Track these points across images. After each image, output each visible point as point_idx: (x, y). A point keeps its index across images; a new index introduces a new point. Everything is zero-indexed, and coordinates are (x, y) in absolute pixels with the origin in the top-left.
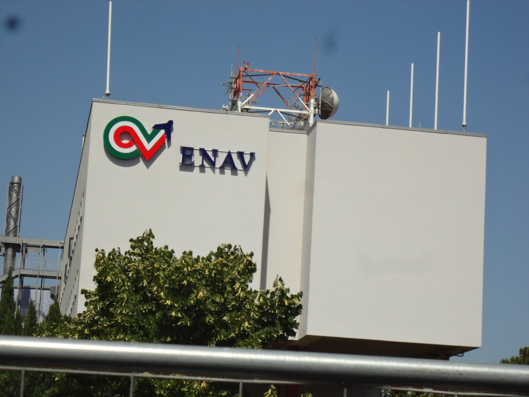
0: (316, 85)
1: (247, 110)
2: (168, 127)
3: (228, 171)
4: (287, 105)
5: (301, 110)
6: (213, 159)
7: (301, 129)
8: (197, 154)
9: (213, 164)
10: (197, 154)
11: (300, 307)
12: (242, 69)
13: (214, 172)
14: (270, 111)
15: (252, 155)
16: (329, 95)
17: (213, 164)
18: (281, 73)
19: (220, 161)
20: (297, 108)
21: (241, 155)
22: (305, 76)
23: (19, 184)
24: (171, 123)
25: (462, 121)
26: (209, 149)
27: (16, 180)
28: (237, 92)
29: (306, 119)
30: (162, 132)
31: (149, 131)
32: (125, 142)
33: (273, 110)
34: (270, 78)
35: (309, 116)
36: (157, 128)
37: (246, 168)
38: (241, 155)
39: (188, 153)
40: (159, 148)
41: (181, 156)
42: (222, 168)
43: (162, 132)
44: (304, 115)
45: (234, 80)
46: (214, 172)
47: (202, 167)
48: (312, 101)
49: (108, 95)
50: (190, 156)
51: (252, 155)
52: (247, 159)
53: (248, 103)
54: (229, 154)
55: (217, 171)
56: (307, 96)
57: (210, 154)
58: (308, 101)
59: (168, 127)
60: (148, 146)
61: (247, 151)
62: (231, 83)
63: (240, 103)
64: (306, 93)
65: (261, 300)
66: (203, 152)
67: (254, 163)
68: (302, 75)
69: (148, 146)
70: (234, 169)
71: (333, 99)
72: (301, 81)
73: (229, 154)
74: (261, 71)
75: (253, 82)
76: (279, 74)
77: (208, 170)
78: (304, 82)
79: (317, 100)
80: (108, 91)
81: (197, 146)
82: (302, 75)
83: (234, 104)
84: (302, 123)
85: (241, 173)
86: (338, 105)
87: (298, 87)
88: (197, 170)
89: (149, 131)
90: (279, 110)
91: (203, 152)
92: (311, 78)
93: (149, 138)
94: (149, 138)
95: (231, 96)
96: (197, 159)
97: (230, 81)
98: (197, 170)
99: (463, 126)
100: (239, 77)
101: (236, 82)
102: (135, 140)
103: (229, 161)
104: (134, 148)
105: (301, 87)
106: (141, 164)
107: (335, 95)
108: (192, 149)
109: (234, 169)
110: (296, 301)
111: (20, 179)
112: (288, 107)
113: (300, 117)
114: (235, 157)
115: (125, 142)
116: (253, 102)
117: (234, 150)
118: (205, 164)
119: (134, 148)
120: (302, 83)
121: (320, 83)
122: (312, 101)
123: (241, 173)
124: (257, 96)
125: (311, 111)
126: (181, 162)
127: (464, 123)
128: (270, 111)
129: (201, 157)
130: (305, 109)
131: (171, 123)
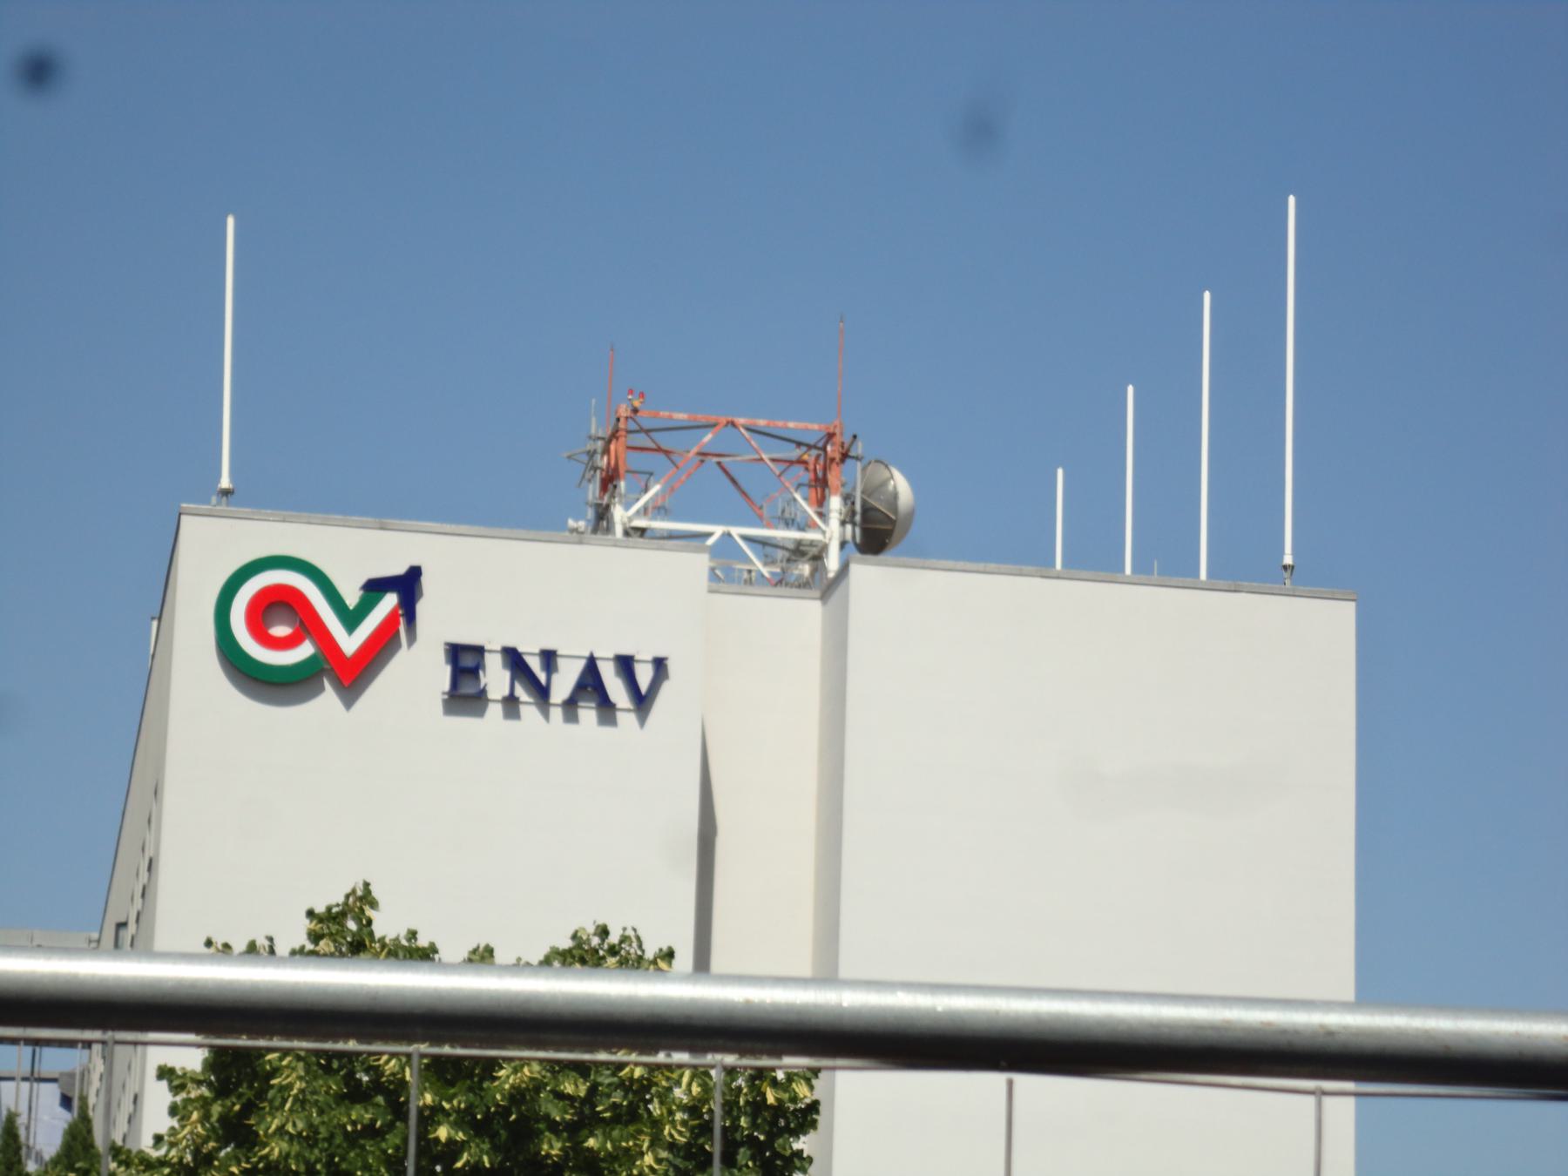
0: (845, 456)
1: (642, 532)
2: (408, 585)
3: (588, 714)
4: (761, 517)
5: (801, 529)
6: (542, 677)
7: (804, 584)
9: (542, 693)
11: (814, 1107)
12: (624, 411)
13: (546, 715)
14: (709, 535)
15: (660, 664)
16: (884, 483)
17: (542, 693)
18: (741, 421)
19: (563, 685)
20: (789, 523)
21: (625, 664)
22: (812, 429)
24: (414, 574)
25: (1282, 553)
26: (530, 650)
28: (609, 481)
29: (818, 557)
30: (390, 601)
31: (352, 598)
33: (718, 530)
34: (708, 437)
35: (824, 548)
36: (375, 587)
37: (642, 702)
39: (467, 661)
40: (382, 646)
41: (446, 672)
42: (571, 705)
43: (390, 601)
44: (812, 544)
45: (600, 444)
46: (546, 715)
47: (511, 703)
48: (835, 503)
49: (226, 493)
50: (474, 672)
51: (660, 664)
52: (644, 675)
53: (645, 511)
54: (591, 665)
55: (556, 713)
56: (820, 487)
57: (535, 664)
58: (821, 502)
59: (408, 585)
60: (350, 643)
61: (643, 655)
62: (591, 454)
63: (620, 515)
64: (816, 479)
65: (696, 1089)
66: (514, 659)
67: (666, 689)
68: (801, 425)
69: (350, 643)
70: (606, 707)
71: (895, 496)
72: (799, 444)
73: (591, 665)
74: (681, 416)
75: (659, 449)
76: (733, 424)
77: (529, 711)
78: (810, 447)
79: (848, 499)
80: (225, 483)
81: (493, 639)
82: (801, 425)
83: (602, 516)
84: (805, 569)
86: (911, 515)
87: (791, 463)
88: (495, 711)
89: (352, 598)
90: (736, 531)
91: (514, 659)
92: (831, 436)
93: (351, 619)
94: (351, 619)
95: (593, 490)
96: (496, 678)
97: (590, 446)
98: (495, 711)
99: (1285, 567)
100: (614, 435)
101: (606, 451)
102: (310, 625)
103: (590, 684)
104: (306, 650)
105: (800, 461)
106: (329, 697)
107: (901, 485)
108: (479, 651)
109: (606, 707)
110: (801, 1089)
112: (761, 521)
113: (798, 551)
115: (281, 631)
116: (658, 509)
117: (605, 654)
118: (520, 692)
119: (306, 650)
120: (804, 449)
121: (859, 449)
122: (835, 503)
123: (627, 719)
124: (670, 489)
125: (832, 531)
126: (446, 686)
127: (1288, 560)
128: (709, 535)
129: (507, 675)
130: (814, 526)
131: (414, 574)
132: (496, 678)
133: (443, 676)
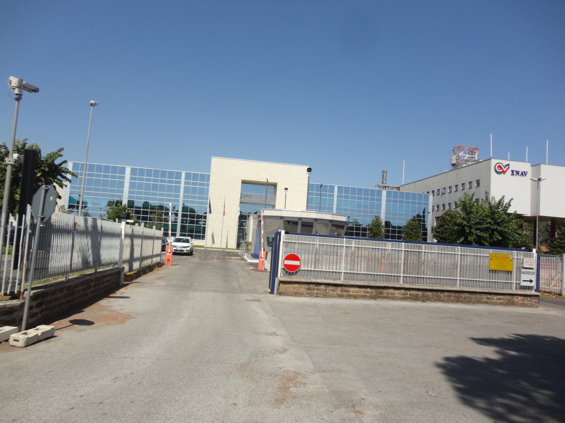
2: (508, 165)
3: (522, 176)
8: (515, 172)
10: (515, 172)
14: (466, 156)
23: (386, 171)
26: (517, 171)
27: (385, 170)
30: (507, 166)
32: (499, 169)
36: (507, 165)
37: (526, 175)
38: (524, 172)
40: (507, 170)
42: (520, 175)
50: (513, 172)
51: (527, 172)
52: (526, 173)
60: (505, 170)
69: (505, 170)
73: (522, 172)
74: (465, 146)
77: (517, 175)
85: (524, 176)
88: (515, 175)
91: (516, 171)
93: (505, 168)
96: (515, 173)
98: (515, 175)
102: (502, 168)
103: (522, 174)
104: (501, 170)
108: (514, 171)
111: (386, 170)
114: (523, 172)
115: (499, 169)
117: (523, 171)
119: (501, 170)
128: (466, 156)
132: (515, 173)
133: (511, 173)
